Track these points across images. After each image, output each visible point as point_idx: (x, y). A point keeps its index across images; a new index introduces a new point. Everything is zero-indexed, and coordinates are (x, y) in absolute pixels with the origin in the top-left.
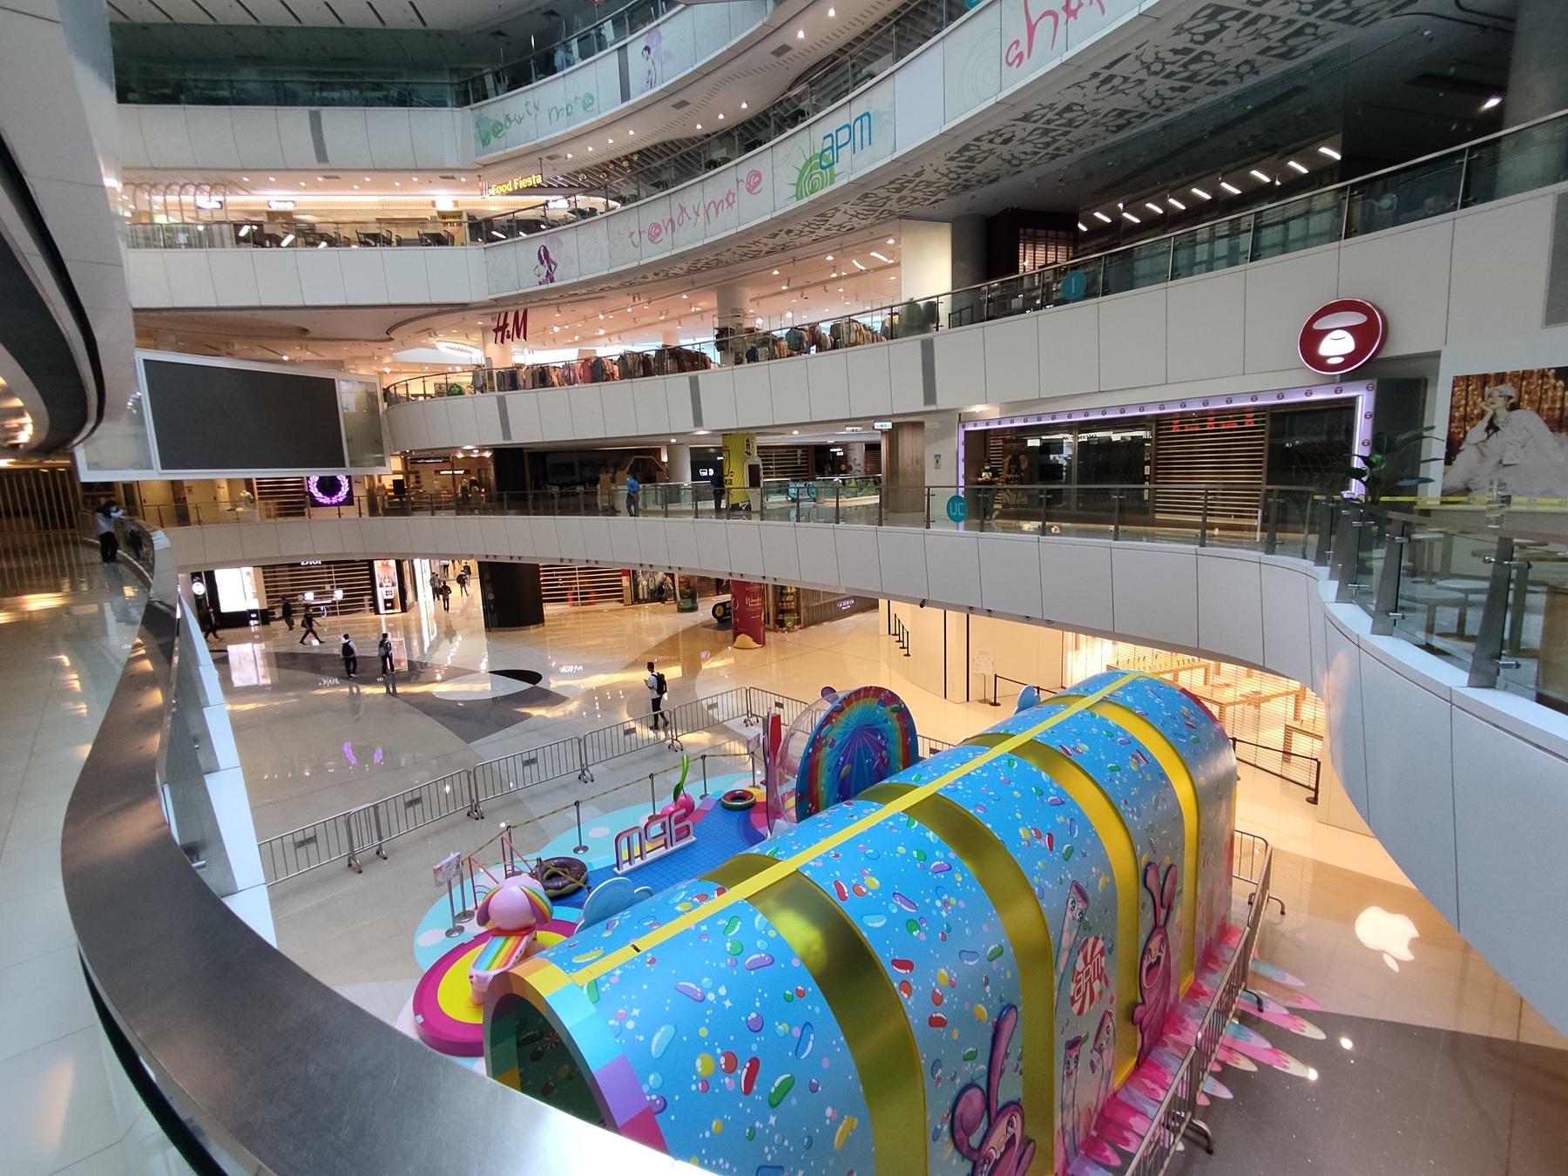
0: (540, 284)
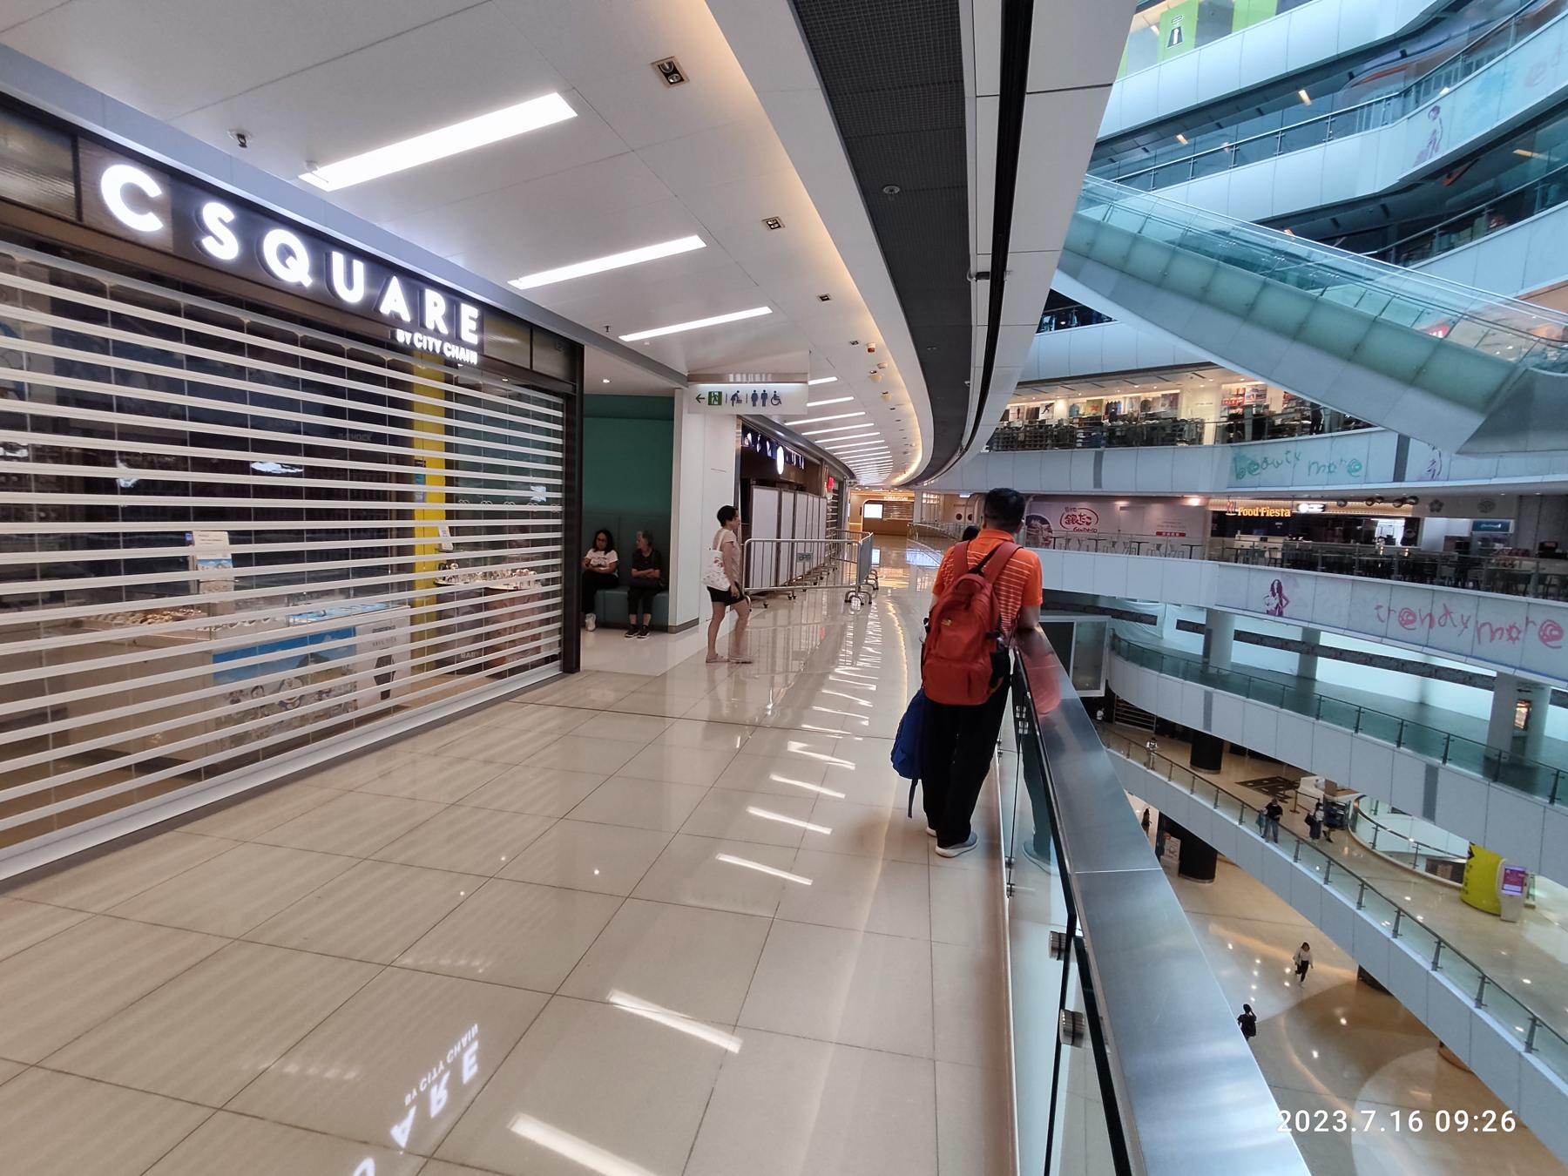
0: (1268, 613)
